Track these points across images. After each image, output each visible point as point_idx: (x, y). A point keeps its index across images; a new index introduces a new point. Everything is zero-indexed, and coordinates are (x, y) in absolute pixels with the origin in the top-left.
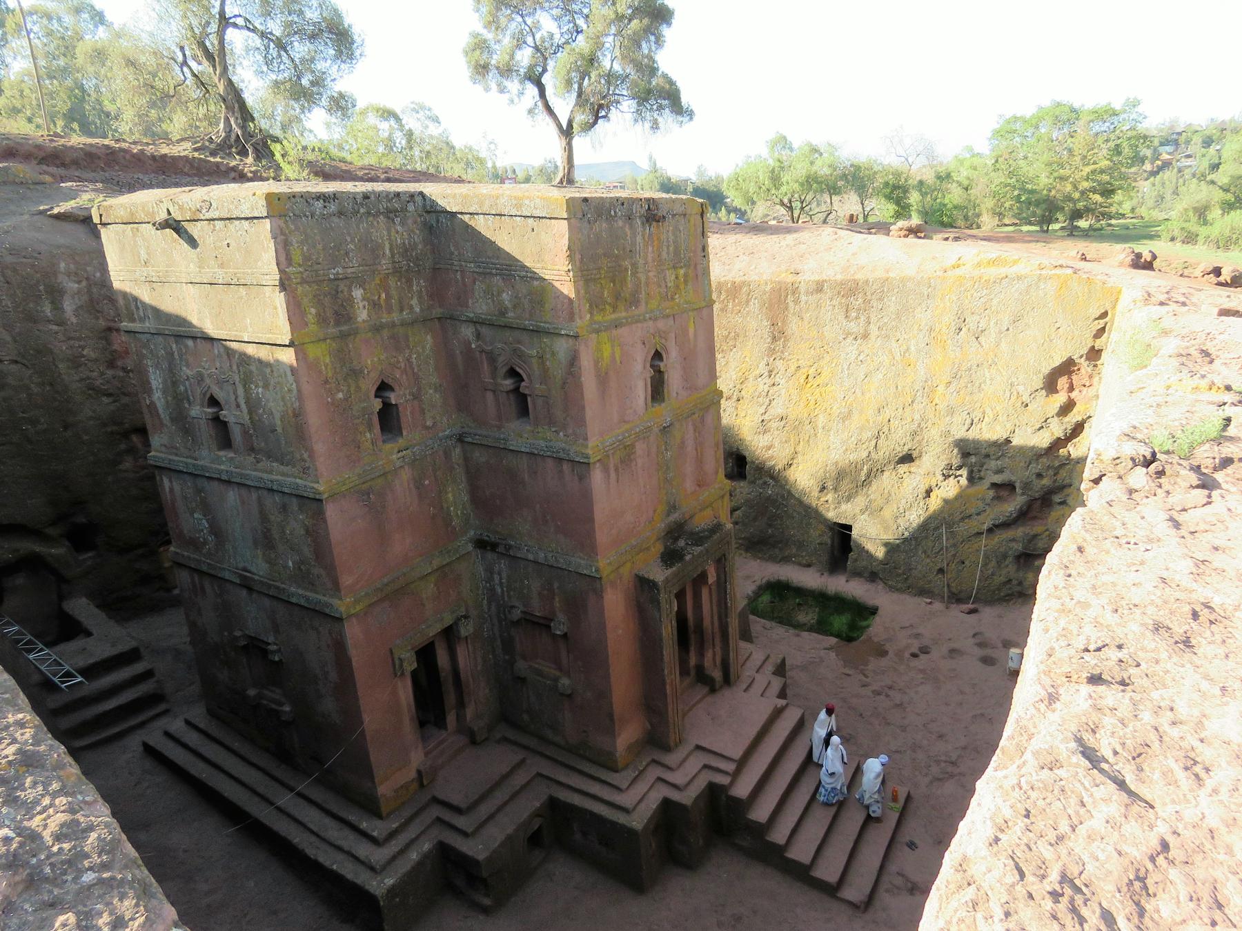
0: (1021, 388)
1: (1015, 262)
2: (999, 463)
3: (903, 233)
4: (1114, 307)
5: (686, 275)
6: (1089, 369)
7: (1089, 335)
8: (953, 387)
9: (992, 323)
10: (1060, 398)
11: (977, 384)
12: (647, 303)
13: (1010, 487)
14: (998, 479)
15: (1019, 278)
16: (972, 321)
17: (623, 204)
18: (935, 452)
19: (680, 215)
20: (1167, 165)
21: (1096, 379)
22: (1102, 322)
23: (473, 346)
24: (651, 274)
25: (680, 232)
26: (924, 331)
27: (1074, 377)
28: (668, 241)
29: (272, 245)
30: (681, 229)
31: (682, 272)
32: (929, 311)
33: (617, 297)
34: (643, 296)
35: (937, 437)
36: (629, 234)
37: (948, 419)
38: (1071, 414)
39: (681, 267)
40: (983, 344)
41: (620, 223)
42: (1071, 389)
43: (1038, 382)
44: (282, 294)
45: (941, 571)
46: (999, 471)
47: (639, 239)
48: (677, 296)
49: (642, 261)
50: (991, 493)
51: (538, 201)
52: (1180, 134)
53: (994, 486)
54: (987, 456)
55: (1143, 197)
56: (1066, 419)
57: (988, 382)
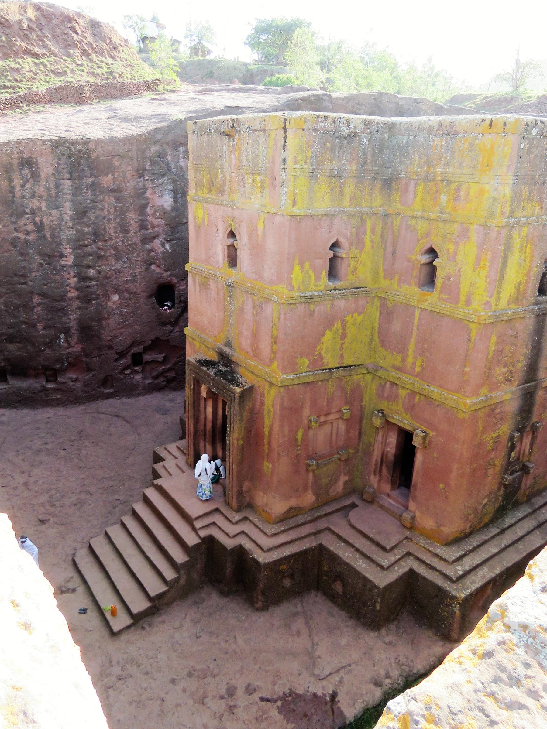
5: (262, 182)
12: (229, 195)
17: (215, 124)
19: (261, 130)
24: (233, 174)
25: (259, 145)
28: (247, 152)
30: (261, 142)
31: (259, 178)
33: (212, 184)
34: (227, 188)
36: (219, 144)
39: (259, 174)
41: (215, 136)
47: (225, 148)
48: (252, 197)
49: (226, 164)
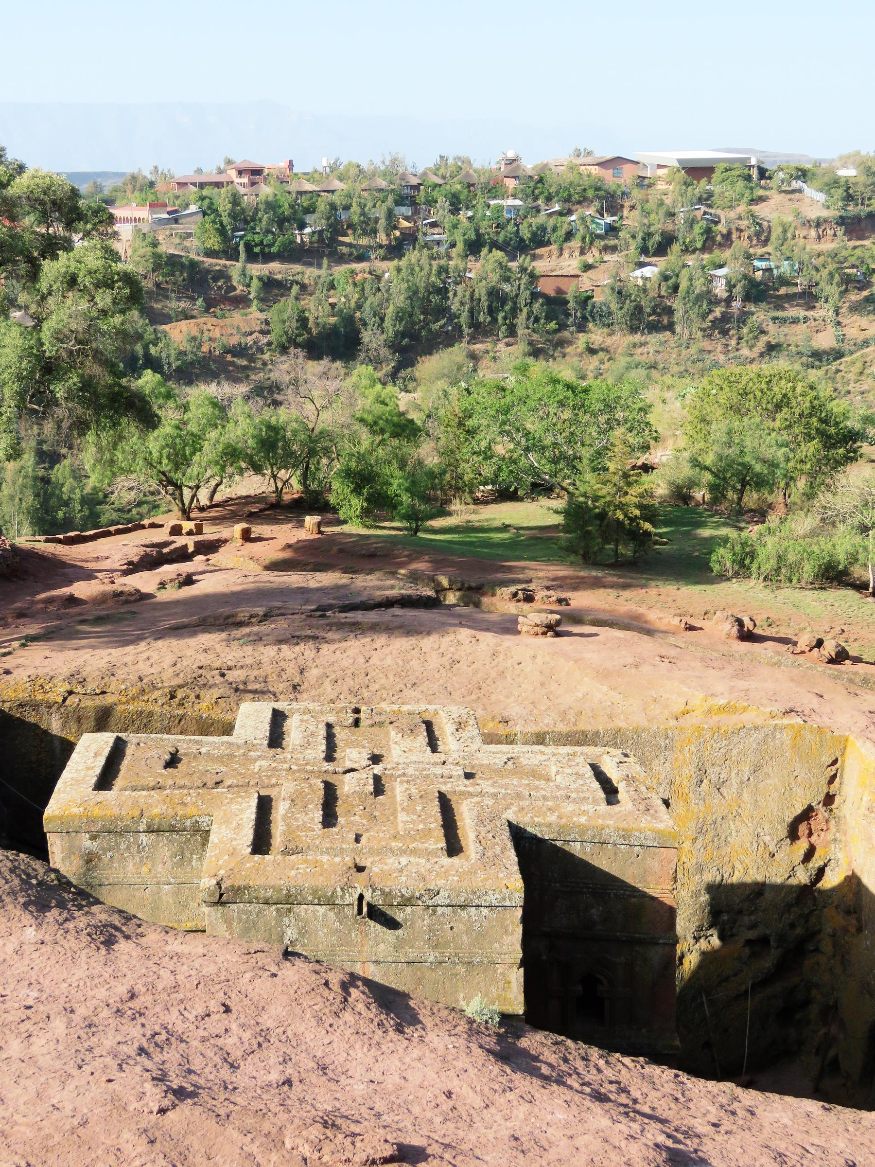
0: (767, 839)
1: (745, 709)
2: (753, 918)
3: (540, 630)
4: (843, 755)
6: (826, 815)
7: (824, 781)
8: (699, 844)
9: (733, 775)
10: (802, 845)
11: (723, 838)
13: (763, 941)
14: (751, 935)
15: (756, 728)
16: (713, 772)
18: (685, 915)
20: (410, 238)
21: (832, 823)
22: (834, 768)
23: (544, 957)
26: (664, 785)
27: (812, 822)
29: (519, 930)
32: (667, 764)
35: (687, 899)
37: (697, 877)
38: (814, 859)
40: (725, 794)
42: (810, 834)
43: (783, 831)
44: (522, 970)
45: (707, 1045)
46: (753, 927)
50: (747, 951)
51: (648, 833)
52: (416, 188)
53: (749, 942)
54: (740, 912)
55: (388, 291)
56: (811, 865)
57: (734, 834)
